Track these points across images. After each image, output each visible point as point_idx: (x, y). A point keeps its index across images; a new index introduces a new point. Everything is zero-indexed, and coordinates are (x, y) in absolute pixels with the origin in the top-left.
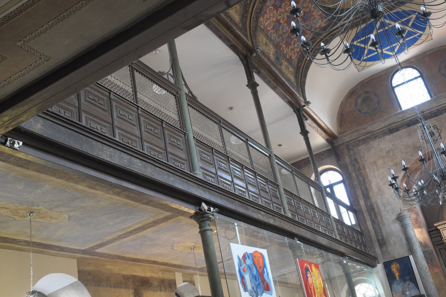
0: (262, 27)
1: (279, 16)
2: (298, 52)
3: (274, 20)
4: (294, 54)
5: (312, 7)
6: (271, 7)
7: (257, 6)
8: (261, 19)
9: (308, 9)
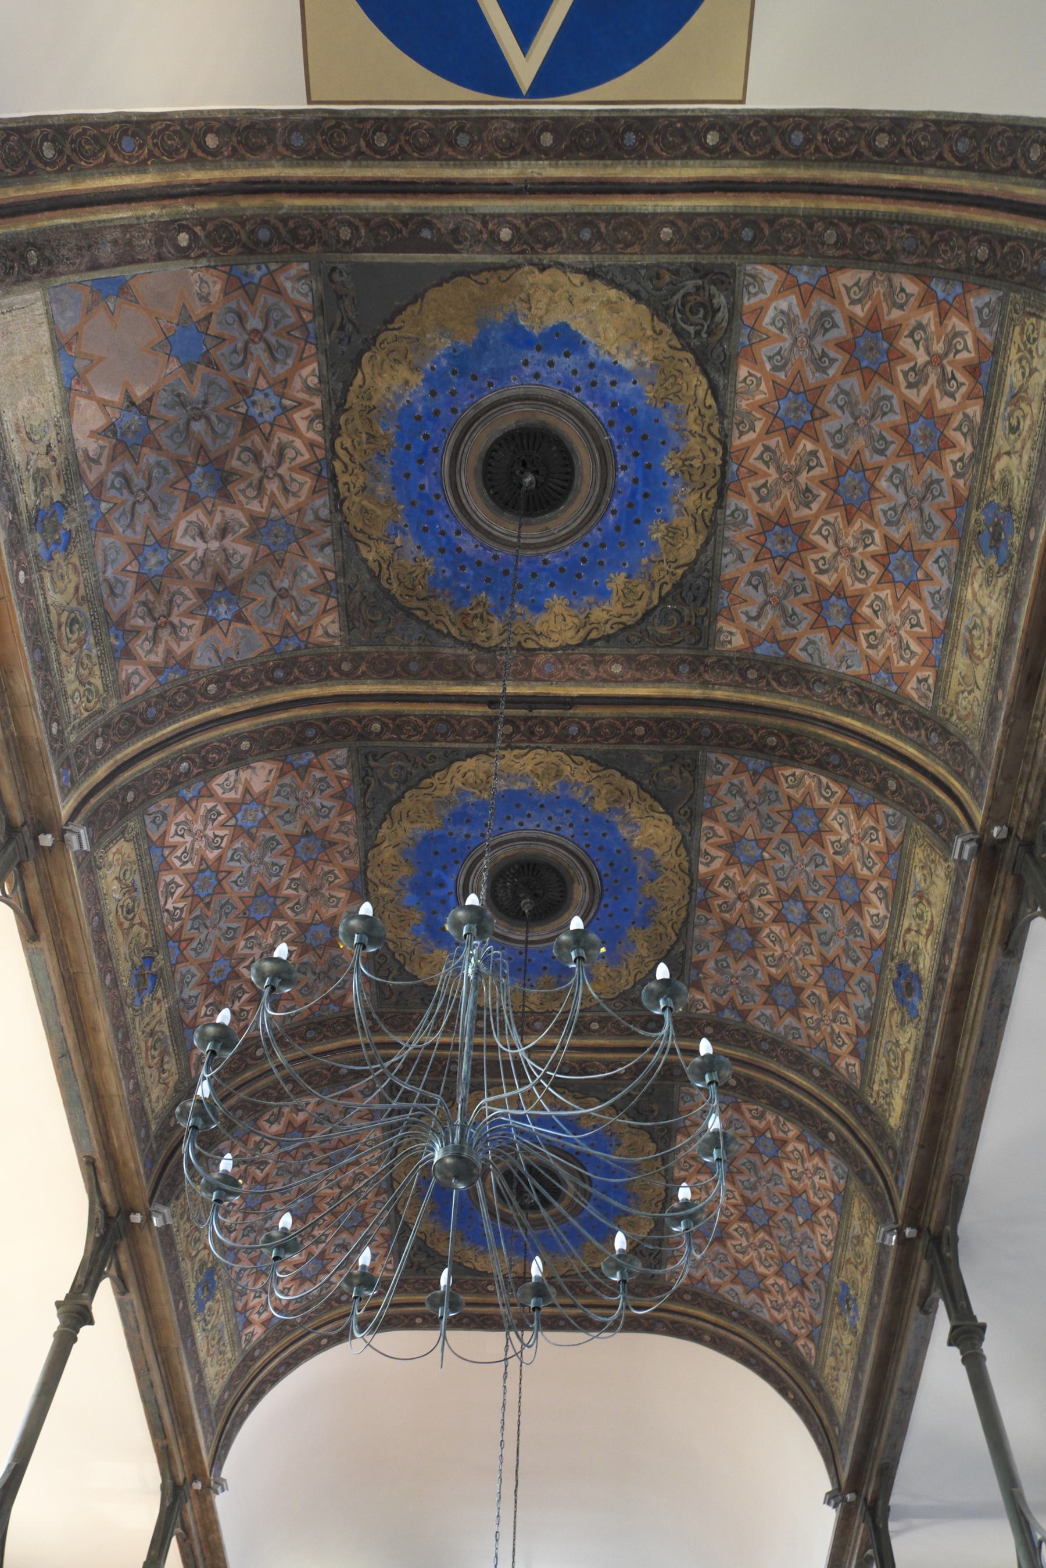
0: (929, 673)
1: (868, 574)
2: (942, 317)
3: (886, 593)
4: (950, 347)
5: (751, 436)
6: (864, 644)
7: (886, 729)
8: (911, 688)
9: (772, 443)
